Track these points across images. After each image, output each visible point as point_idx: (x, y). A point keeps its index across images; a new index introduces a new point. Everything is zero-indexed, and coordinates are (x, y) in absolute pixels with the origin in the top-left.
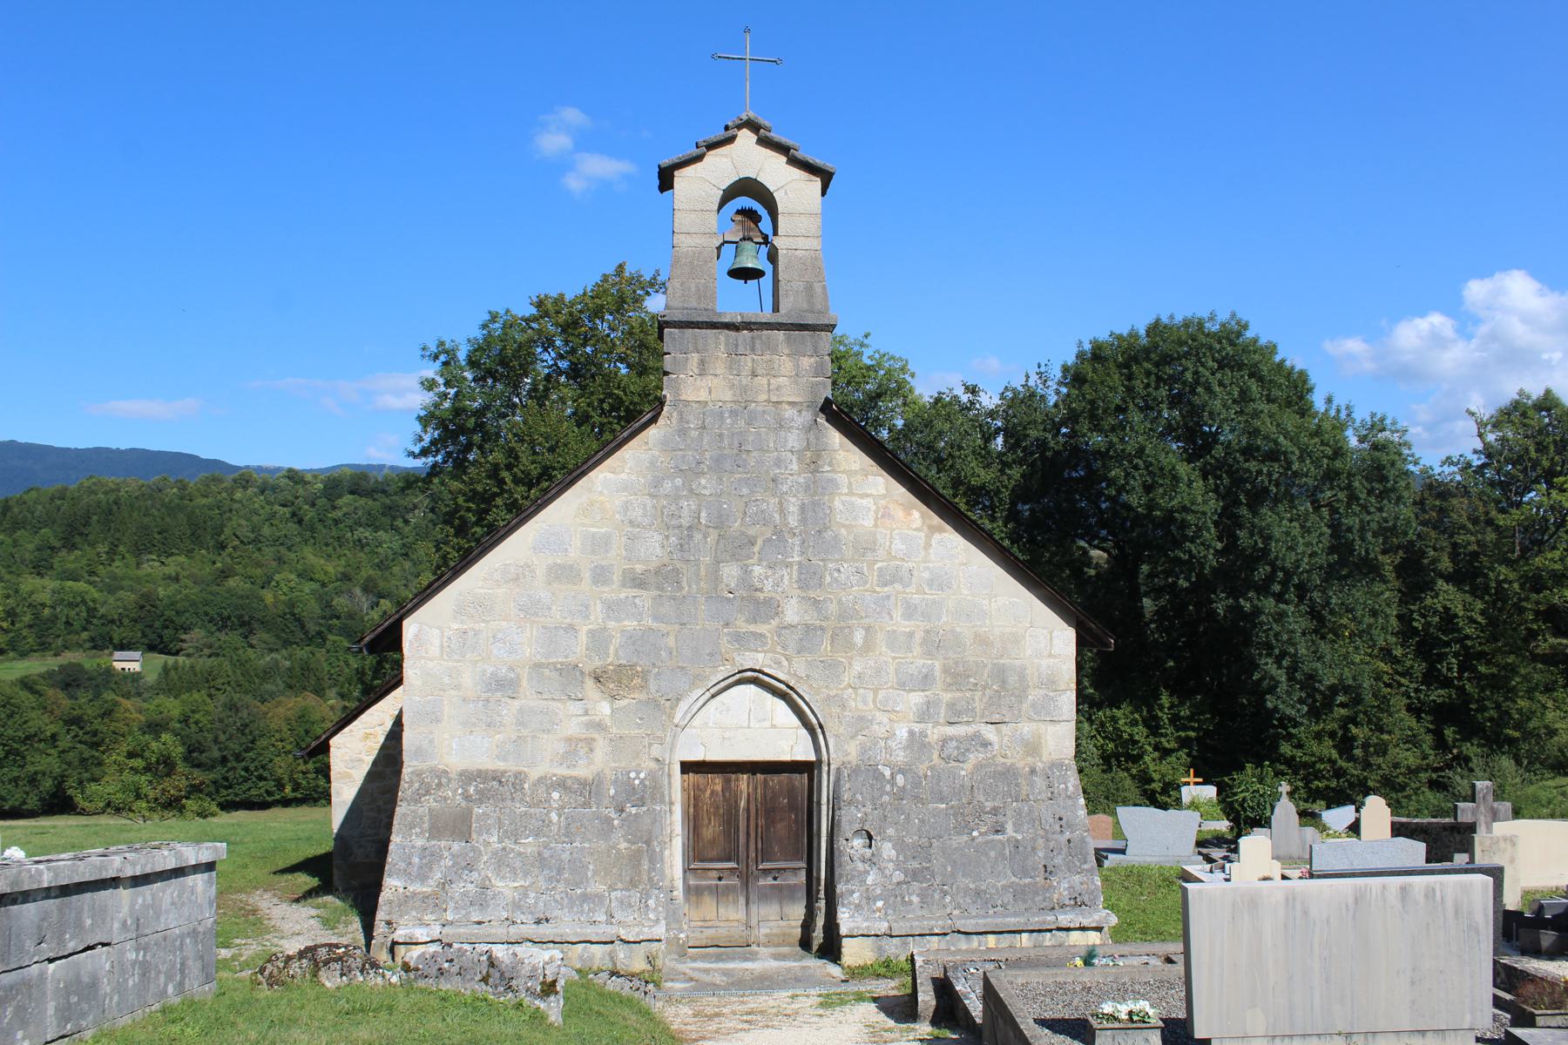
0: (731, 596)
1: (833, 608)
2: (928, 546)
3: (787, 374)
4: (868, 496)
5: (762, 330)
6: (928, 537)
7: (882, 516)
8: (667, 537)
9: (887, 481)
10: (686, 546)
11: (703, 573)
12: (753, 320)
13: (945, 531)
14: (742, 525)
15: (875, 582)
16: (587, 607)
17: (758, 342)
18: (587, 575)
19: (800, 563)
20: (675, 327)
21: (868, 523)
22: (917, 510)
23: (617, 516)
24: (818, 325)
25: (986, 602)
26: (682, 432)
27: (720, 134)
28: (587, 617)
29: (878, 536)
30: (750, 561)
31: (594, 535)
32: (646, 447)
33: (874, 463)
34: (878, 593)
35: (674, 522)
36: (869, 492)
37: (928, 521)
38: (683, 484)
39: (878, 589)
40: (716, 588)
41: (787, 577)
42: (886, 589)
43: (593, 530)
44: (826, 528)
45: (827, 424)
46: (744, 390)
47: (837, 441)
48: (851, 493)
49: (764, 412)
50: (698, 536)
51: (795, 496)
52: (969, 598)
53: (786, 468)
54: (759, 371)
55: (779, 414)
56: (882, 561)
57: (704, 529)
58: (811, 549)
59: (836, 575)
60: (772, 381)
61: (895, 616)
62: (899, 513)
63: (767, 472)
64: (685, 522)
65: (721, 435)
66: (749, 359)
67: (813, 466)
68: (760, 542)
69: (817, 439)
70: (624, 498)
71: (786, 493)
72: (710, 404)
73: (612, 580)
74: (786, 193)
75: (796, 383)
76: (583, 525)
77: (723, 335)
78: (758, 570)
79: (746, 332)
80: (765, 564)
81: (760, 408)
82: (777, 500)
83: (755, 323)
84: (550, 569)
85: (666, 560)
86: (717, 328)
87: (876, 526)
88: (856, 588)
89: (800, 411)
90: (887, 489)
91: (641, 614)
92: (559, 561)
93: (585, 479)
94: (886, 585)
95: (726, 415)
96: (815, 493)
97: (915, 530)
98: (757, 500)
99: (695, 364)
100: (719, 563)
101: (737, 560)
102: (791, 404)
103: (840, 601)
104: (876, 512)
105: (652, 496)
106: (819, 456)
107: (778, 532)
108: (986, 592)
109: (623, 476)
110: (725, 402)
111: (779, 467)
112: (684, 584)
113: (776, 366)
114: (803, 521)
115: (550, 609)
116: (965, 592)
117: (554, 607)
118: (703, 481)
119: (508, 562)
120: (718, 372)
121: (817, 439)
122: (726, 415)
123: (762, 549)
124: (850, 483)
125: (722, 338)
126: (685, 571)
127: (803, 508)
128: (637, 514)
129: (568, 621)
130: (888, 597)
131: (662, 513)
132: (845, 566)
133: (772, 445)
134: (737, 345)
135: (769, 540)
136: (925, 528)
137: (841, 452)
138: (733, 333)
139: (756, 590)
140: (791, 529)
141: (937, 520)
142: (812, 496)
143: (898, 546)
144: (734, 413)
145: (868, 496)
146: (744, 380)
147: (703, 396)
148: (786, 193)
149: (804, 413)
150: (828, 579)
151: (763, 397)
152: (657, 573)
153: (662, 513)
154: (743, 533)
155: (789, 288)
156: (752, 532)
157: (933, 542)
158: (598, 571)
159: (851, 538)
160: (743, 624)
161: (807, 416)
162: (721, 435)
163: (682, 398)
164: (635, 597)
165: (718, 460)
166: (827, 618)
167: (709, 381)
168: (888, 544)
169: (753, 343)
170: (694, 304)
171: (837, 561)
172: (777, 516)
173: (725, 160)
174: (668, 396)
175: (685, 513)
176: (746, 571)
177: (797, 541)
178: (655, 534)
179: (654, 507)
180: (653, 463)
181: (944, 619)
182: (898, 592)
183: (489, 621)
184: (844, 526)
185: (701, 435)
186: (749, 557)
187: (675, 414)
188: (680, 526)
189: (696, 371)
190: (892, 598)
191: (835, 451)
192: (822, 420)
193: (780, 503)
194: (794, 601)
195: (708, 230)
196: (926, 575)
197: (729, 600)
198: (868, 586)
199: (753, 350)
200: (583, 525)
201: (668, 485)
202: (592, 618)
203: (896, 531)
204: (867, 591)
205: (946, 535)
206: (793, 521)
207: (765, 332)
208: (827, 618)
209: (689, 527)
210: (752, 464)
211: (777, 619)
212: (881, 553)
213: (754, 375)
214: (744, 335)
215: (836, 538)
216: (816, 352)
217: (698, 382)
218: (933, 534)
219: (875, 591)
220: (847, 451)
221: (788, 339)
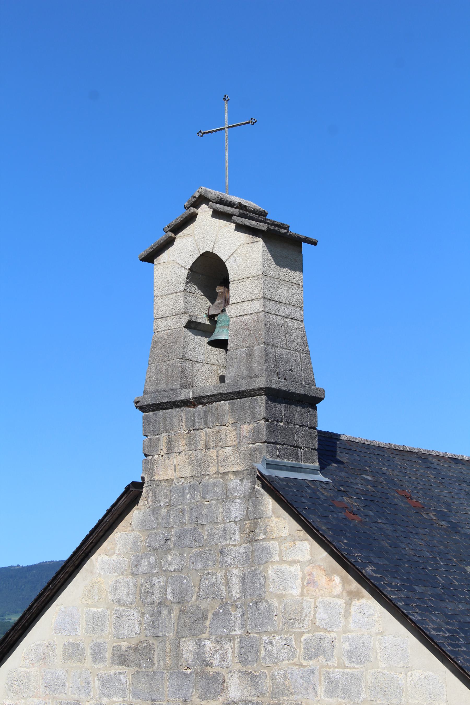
0: (189, 671)
1: (267, 683)
2: (347, 614)
3: (232, 443)
4: (295, 562)
5: (211, 403)
6: (348, 604)
7: (308, 584)
8: (143, 613)
9: (311, 545)
10: (156, 623)
11: (168, 649)
12: (201, 395)
13: (362, 597)
14: (197, 599)
15: (302, 655)
16: (88, 683)
17: (209, 415)
18: (89, 653)
19: (240, 637)
20: (149, 411)
21: (295, 591)
22: (338, 575)
23: (110, 596)
24: (251, 390)
25: (402, 676)
26: (155, 511)
27: (180, 214)
28: (88, 693)
29: (305, 605)
30: (203, 636)
31: (94, 614)
32: (130, 529)
33: (300, 528)
34: (304, 666)
35: (149, 600)
36: (296, 558)
37: (347, 587)
38: (156, 562)
39: (304, 663)
40: (177, 664)
41: (230, 651)
42: (311, 662)
43: (94, 610)
44: (261, 599)
45: (263, 491)
46: (200, 463)
47: (270, 507)
48: (281, 561)
49: (214, 484)
50: (165, 612)
51: (237, 567)
52: (386, 671)
53: (231, 539)
54: (212, 444)
55: (225, 485)
56: (308, 632)
57: (169, 604)
58: (249, 622)
59: (269, 648)
60: (220, 452)
61: (319, 694)
62: (322, 579)
63: (217, 544)
64: (156, 599)
65: (183, 511)
66: (203, 432)
67: (252, 535)
68: (210, 616)
69: (254, 506)
70: (114, 579)
71: (230, 565)
72: (175, 481)
73: (105, 658)
74: (235, 261)
75: (238, 451)
76: (87, 605)
77: (184, 412)
78: (208, 644)
79: (200, 406)
80: (213, 638)
81: (212, 481)
82: (223, 572)
83: (203, 397)
84: (65, 648)
85: (143, 637)
86: (178, 406)
87: (302, 594)
88: (286, 662)
89: (241, 480)
90: (311, 554)
91: (124, 690)
92: (71, 641)
93: (88, 562)
94: (311, 658)
95: (187, 491)
96: (253, 564)
97: (336, 597)
98: (208, 574)
99: (165, 444)
100: (180, 638)
101: (193, 635)
102: (235, 473)
103: (273, 676)
104: (303, 579)
105: (134, 575)
106: (256, 524)
107: (224, 604)
108: (402, 664)
109: (115, 557)
110: (185, 478)
111: (225, 538)
112: (155, 660)
113: (223, 436)
114: (244, 592)
115: (64, 685)
116: (382, 665)
117: (67, 684)
118: (169, 558)
119: (39, 643)
120: (181, 449)
121: (254, 506)
122: (187, 491)
123: (211, 623)
124: (281, 551)
125: (184, 416)
126: (156, 648)
127: (243, 579)
128: (123, 593)
129: (76, 697)
130: (313, 671)
131: (141, 590)
132: (277, 637)
133: (220, 517)
134: (194, 421)
135: (216, 614)
136: (345, 595)
137: (273, 518)
138: (191, 409)
139: (207, 665)
140: (235, 601)
141: (355, 585)
142: (250, 566)
143: (322, 615)
144: (192, 488)
145: (295, 562)
146: (199, 454)
147: (170, 474)
148: (235, 261)
149: (245, 481)
150: (263, 653)
151: (213, 470)
152: (136, 649)
153: (141, 590)
154: (198, 608)
155: (234, 356)
156: (204, 606)
157: (352, 610)
158: (96, 650)
159: (282, 608)
160: (198, 700)
161: (247, 483)
162: (183, 511)
163: (156, 478)
164: (120, 673)
165: (180, 536)
166: (262, 695)
167: (176, 459)
168: (312, 613)
169: (206, 416)
170: (163, 386)
171: (270, 633)
172: (223, 588)
173: (190, 239)
174: (146, 478)
175: (157, 590)
176: (200, 647)
177: (238, 613)
178: (135, 612)
179: (135, 585)
180: (134, 543)
181: (363, 696)
182: (322, 666)
183: (26, 698)
184: (277, 596)
185: (169, 512)
186: (202, 632)
187: (150, 494)
188: (153, 603)
189: (165, 450)
190: (317, 673)
191: (269, 518)
192: (258, 487)
193: (226, 575)
194: (235, 676)
195: (178, 311)
196: (346, 646)
197: (186, 675)
198: (296, 659)
199: (206, 424)
200: (87, 605)
201: (145, 563)
202: (92, 694)
203: (320, 599)
204: (295, 664)
205: (363, 601)
206: (236, 593)
207: (215, 404)
208: (262, 695)
209: (160, 604)
210: (205, 538)
211: (224, 695)
212: (307, 623)
213: (207, 448)
214: (199, 410)
215: (269, 608)
216: (254, 418)
217: (167, 461)
218: (352, 601)
219: (301, 665)
220: (278, 517)
221: (232, 408)
